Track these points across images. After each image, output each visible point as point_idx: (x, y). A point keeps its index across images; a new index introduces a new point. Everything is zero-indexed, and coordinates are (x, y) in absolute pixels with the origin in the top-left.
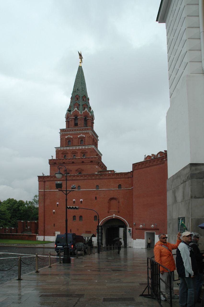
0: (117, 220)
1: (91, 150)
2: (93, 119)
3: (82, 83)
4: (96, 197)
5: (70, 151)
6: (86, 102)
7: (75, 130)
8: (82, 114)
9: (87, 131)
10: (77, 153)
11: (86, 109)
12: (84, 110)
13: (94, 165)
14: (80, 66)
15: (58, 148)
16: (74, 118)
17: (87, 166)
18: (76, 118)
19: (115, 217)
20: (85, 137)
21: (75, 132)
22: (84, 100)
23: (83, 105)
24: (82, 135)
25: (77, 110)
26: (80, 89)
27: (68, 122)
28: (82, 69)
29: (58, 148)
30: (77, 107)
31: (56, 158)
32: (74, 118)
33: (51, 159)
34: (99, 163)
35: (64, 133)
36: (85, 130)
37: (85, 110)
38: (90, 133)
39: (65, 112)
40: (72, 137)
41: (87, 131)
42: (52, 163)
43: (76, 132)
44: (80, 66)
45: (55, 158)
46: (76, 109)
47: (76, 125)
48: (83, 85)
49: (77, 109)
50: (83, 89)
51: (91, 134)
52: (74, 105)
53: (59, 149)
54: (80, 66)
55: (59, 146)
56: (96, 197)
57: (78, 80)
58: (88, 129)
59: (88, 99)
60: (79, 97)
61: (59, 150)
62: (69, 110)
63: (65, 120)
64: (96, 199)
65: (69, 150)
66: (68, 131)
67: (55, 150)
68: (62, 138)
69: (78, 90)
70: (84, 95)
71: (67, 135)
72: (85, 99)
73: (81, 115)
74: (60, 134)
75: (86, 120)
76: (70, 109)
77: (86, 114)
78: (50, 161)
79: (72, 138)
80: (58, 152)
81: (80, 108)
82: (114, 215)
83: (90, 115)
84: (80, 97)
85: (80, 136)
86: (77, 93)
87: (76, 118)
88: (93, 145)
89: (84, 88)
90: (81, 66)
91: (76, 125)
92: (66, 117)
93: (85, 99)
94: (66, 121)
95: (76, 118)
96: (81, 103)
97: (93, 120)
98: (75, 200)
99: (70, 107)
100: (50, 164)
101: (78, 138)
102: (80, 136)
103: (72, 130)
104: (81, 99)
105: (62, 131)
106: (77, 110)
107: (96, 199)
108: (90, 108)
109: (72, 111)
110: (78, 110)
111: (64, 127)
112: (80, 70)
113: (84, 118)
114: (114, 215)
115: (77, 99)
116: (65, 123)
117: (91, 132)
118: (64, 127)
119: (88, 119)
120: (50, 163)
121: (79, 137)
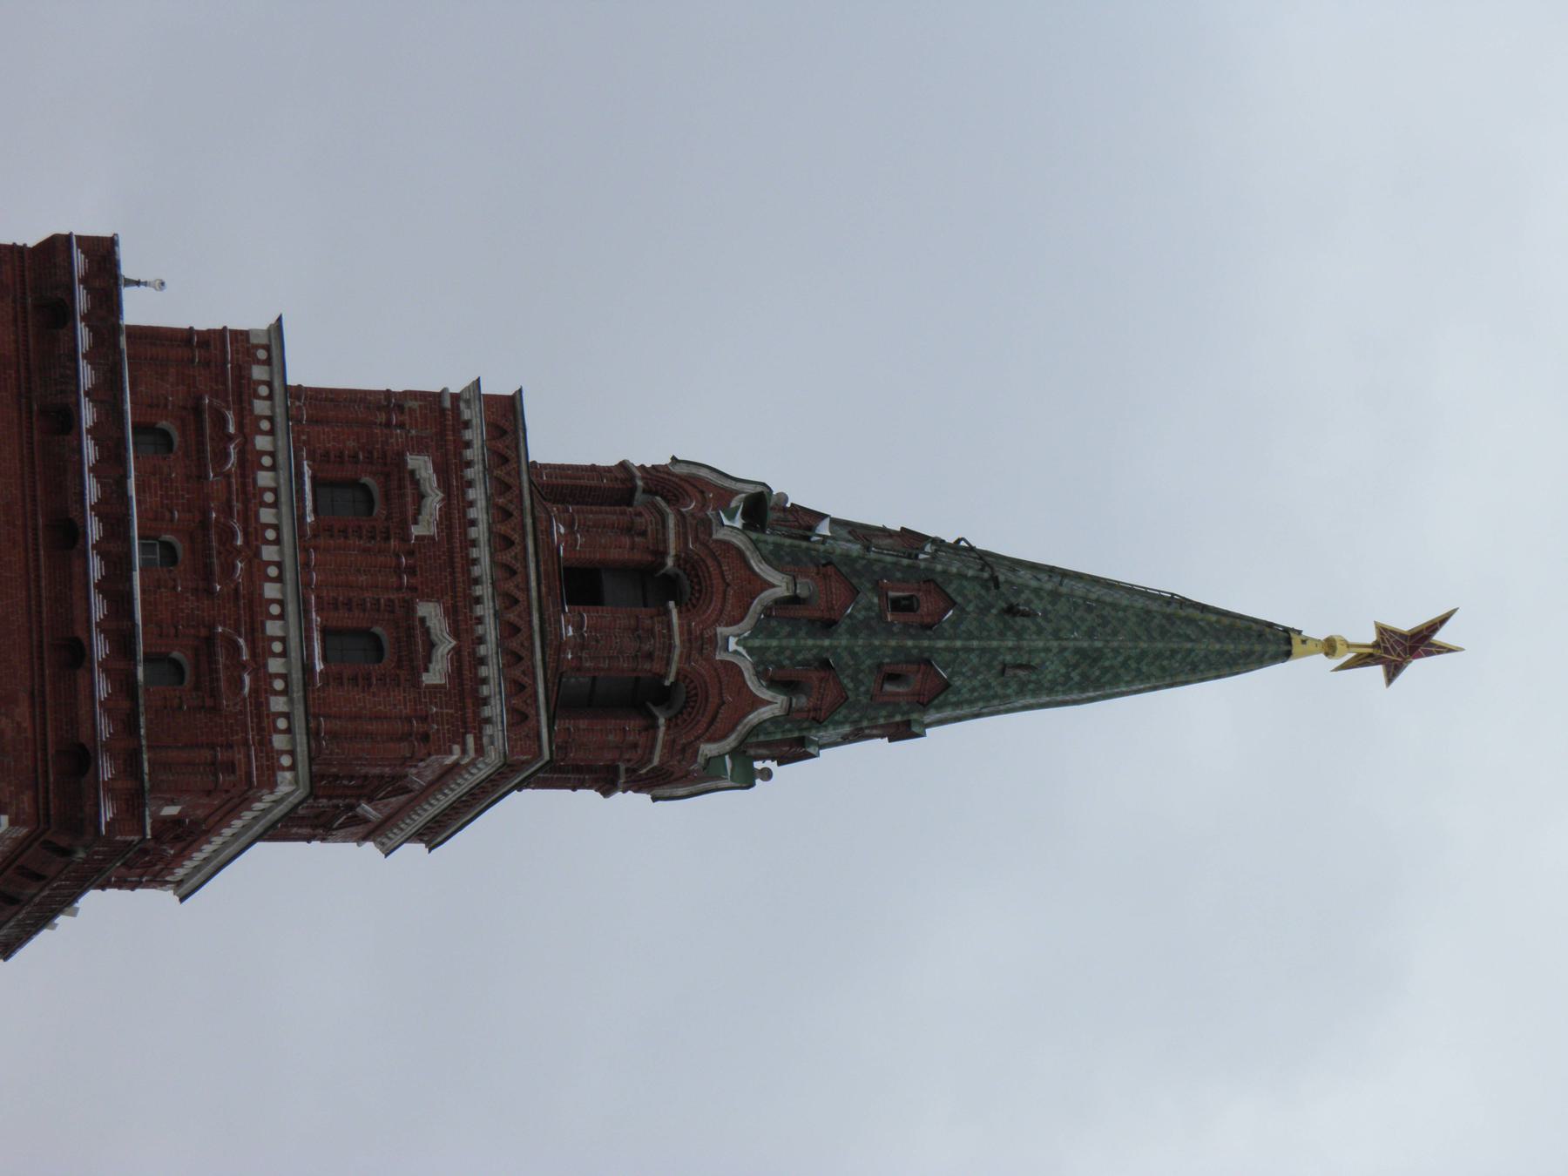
1: (239, 756)
2: (663, 780)
3: (1093, 657)
5: (237, 506)
6: (864, 700)
7: (507, 570)
8: (709, 660)
9: (495, 709)
10: (210, 592)
11: (773, 705)
12: (774, 684)
13: (26, 798)
14: (1289, 641)
16: (670, 562)
17: (22, 711)
18: (656, 584)
20: (416, 682)
21: (483, 569)
22: (893, 678)
23: (825, 665)
25: (767, 596)
27: (611, 490)
28: (1261, 661)
29: (268, 362)
30: (794, 600)
31: (143, 335)
32: (670, 562)
33: (126, 270)
34: (66, 852)
35: (476, 435)
36: (518, 689)
37: (766, 694)
38: (478, 739)
39: (741, 458)
40: (416, 531)
43: (487, 579)
44: (1296, 640)
45: (139, 309)
46: (780, 585)
47: (581, 584)
48: (1075, 676)
49: (781, 602)
50: (1021, 673)
51: (464, 751)
52: (826, 566)
53: (259, 373)
54: (1297, 646)
55: (298, 375)
57: (1123, 621)
58: (519, 717)
59: (902, 731)
60: (929, 627)
62: (760, 506)
63: (649, 453)
66: (502, 486)
67: (254, 320)
68: (401, 408)
69: (1011, 610)
70: (946, 686)
71: (451, 473)
72: (901, 690)
73: (702, 644)
74: (455, 388)
75: (643, 697)
76: (772, 516)
77: (714, 699)
78: (103, 252)
79: (405, 537)
81: (790, 635)
83: (708, 749)
84: (925, 633)
86: (970, 608)
87: (656, 584)
88: (314, 778)
89: (1039, 684)
90: (1287, 655)
91: (581, 584)
92: (677, 470)
93: (901, 690)
94: (623, 465)
95: (670, 588)
96: (844, 642)
97: (639, 784)
99: (805, 519)
101: (410, 608)
103: (516, 537)
105: (506, 414)
106: (767, 596)
108: (795, 750)
109: (755, 543)
110: (767, 610)
111: (547, 444)
113: (665, 676)
115: (897, 605)
116: (608, 460)
117: (480, 750)
119: (655, 727)
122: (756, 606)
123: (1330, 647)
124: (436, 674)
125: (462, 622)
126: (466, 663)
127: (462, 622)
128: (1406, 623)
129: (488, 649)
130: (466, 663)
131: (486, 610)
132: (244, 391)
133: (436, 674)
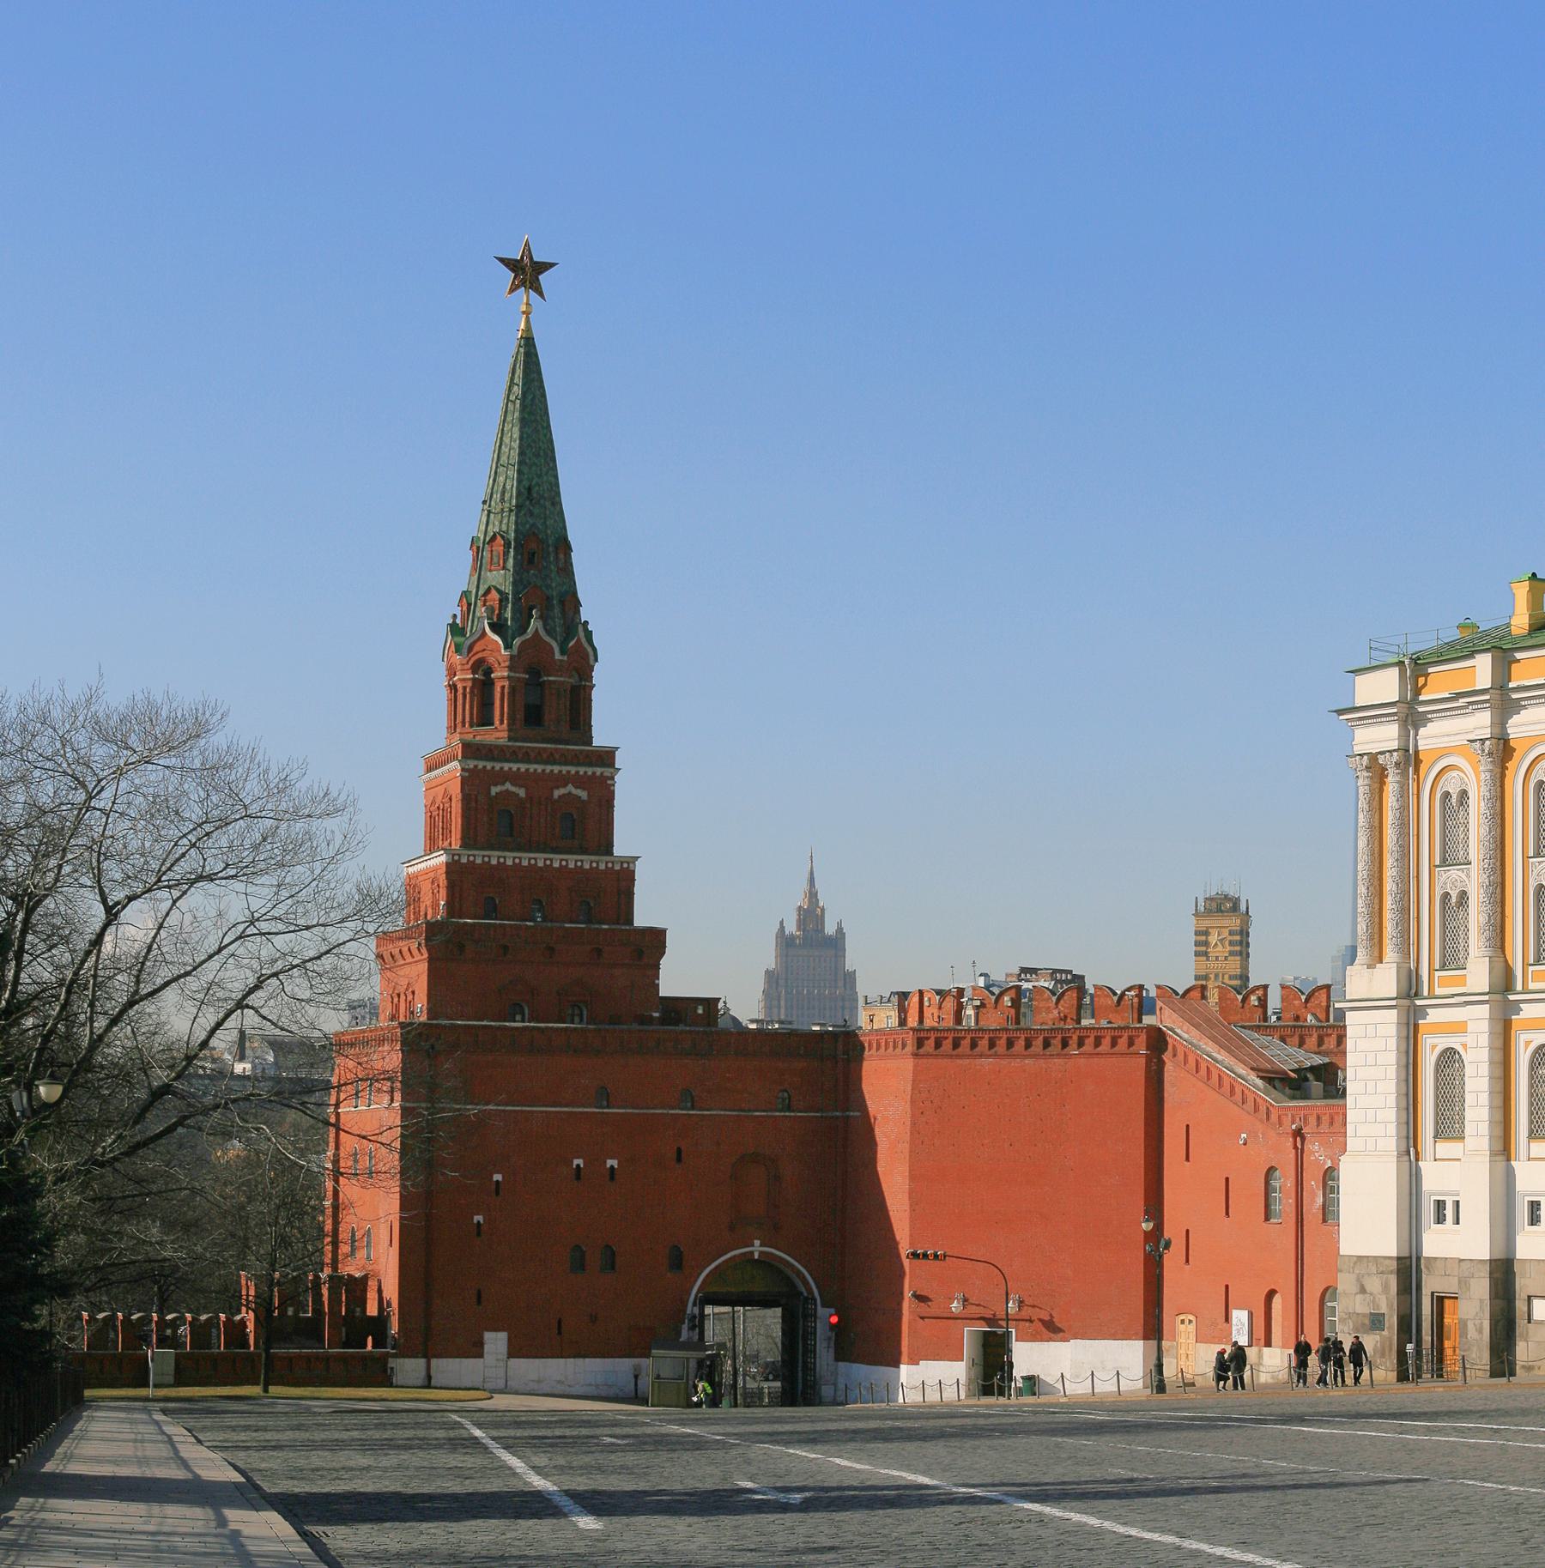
0: (766, 1263)
4: (679, 1151)
7: (538, 757)
9: (599, 771)
19: (761, 1253)
21: (539, 768)
24: (570, 788)
25: (542, 633)
26: (542, 497)
35: (481, 764)
56: (679, 1151)
64: (679, 1160)
65: (517, 867)
82: (757, 1243)
85: (562, 791)
98: (576, 1162)
102: (562, 791)
106: (542, 633)
107: (679, 1160)
110: (548, 632)
112: (528, 342)
114: (757, 1243)
121: (557, 793)
122: (547, 639)
124: (583, 794)
125: (563, 780)
126: (579, 781)
127: (563, 780)
129: (573, 770)
130: (579, 781)
131: (556, 769)
133: (583, 794)
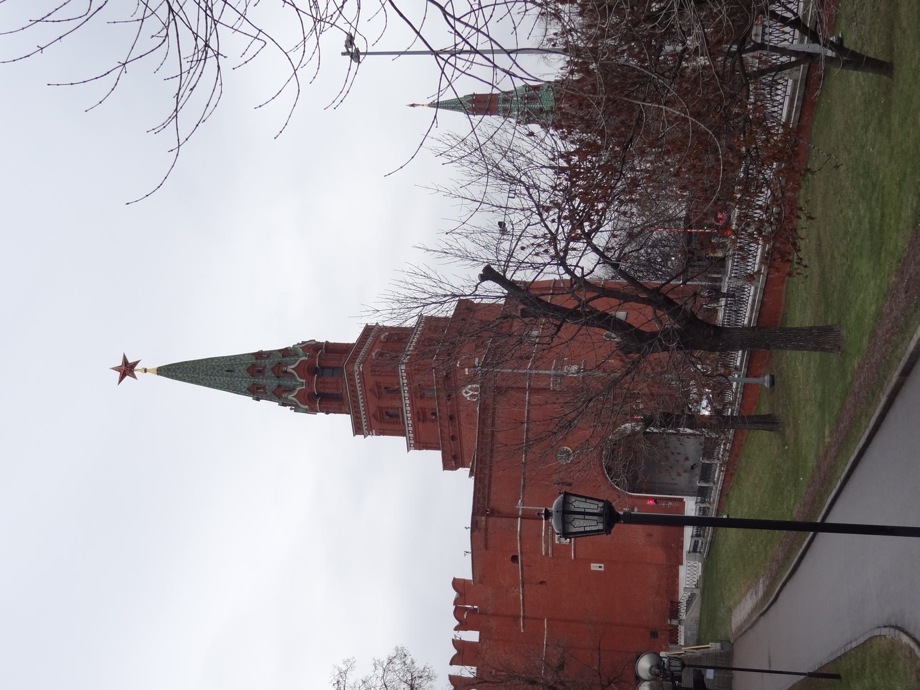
11: (290, 369)
12: (291, 373)
15: (408, 440)
35: (365, 428)
41: (357, 377)
42: (451, 462)
46: (290, 397)
53: (412, 442)
61: (416, 442)
67: (414, 452)
80: (419, 443)
100: (456, 469)
104: (261, 381)
105: (358, 429)
116: (331, 415)
118: (345, 420)
120: (455, 468)
123: (146, 371)
128: (128, 378)
132: (415, 439)
